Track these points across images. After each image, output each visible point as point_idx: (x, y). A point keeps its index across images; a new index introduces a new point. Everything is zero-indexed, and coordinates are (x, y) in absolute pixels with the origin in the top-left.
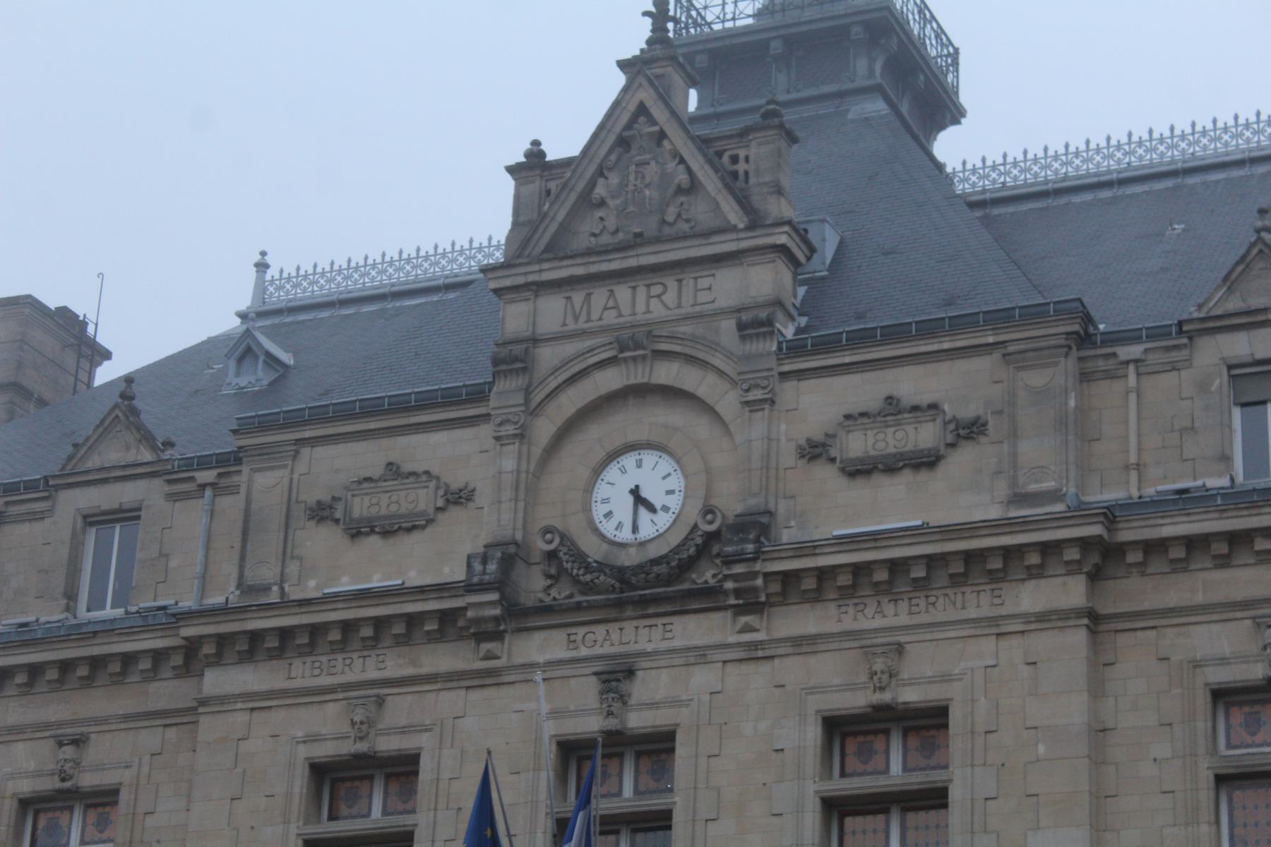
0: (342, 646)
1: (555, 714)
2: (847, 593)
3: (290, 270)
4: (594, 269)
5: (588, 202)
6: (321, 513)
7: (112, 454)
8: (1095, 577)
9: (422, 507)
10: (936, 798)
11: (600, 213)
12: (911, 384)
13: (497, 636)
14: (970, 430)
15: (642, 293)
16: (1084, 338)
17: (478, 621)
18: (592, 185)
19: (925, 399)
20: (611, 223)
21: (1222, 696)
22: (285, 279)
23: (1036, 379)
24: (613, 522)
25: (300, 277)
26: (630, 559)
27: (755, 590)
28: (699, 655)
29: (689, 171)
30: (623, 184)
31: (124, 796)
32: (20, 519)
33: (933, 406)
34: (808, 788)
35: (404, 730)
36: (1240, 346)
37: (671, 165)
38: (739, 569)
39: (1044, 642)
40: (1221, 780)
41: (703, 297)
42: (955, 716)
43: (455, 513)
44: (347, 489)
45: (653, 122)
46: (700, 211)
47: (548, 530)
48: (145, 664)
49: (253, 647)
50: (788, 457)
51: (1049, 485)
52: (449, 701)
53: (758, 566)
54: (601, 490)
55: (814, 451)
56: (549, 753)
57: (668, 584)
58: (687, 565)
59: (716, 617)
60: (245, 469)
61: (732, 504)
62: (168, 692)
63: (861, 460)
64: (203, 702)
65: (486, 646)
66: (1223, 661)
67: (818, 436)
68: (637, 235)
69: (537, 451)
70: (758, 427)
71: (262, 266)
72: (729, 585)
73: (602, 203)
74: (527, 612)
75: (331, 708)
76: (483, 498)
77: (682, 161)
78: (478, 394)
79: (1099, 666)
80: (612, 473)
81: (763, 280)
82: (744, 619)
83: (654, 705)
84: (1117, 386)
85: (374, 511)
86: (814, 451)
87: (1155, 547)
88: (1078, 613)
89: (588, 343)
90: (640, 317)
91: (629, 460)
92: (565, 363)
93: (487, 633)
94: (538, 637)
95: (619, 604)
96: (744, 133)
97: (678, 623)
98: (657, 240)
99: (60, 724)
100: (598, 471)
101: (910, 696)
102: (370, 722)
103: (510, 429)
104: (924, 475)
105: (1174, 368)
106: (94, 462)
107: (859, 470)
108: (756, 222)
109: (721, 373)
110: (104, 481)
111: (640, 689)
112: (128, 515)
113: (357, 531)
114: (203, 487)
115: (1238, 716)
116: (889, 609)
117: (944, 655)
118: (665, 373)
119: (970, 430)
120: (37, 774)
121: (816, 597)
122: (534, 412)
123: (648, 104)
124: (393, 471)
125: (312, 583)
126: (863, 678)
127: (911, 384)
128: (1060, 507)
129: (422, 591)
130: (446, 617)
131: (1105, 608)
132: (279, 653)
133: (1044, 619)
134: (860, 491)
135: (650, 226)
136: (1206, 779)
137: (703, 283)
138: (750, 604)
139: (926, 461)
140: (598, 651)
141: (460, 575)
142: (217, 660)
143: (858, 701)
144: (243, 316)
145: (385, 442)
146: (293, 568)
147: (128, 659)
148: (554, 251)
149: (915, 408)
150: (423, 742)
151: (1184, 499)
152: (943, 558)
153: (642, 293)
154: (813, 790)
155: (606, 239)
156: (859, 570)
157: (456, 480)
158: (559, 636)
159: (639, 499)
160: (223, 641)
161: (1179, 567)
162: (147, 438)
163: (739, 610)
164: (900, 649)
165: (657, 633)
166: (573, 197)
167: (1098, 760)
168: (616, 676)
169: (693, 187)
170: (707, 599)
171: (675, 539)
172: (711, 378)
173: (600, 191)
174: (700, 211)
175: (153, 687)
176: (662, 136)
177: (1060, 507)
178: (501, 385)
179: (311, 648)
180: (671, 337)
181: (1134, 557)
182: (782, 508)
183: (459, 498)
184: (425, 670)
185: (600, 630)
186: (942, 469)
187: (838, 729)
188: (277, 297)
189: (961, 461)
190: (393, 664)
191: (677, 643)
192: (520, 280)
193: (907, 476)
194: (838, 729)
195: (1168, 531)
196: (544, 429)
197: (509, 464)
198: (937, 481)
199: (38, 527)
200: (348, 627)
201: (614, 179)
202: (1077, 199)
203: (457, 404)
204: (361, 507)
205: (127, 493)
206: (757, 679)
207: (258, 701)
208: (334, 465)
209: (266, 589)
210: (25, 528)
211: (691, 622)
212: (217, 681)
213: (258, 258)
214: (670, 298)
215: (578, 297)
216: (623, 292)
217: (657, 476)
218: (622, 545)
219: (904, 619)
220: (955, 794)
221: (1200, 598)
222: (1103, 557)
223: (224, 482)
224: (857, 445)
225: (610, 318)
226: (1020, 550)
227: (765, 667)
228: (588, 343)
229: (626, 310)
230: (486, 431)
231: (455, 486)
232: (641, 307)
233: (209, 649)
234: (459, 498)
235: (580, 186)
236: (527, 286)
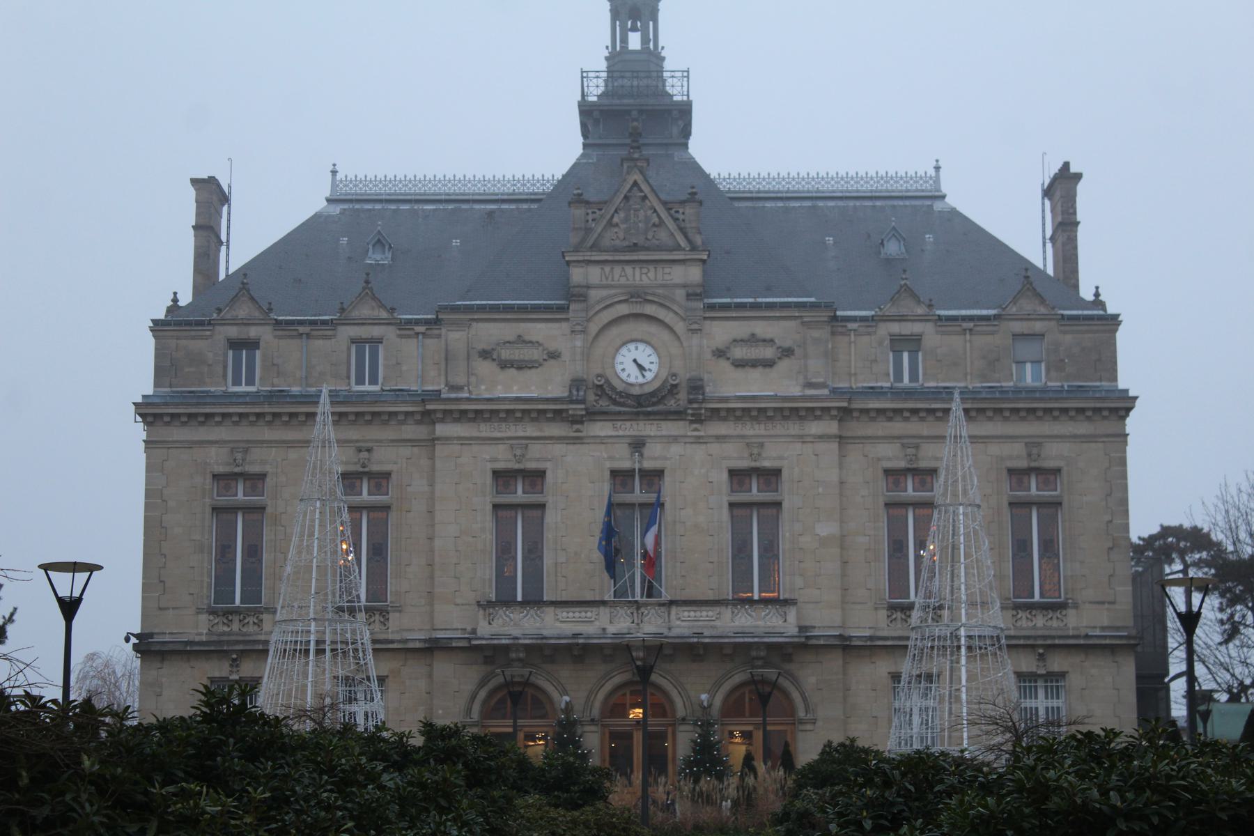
0: (504, 420)
1: (611, 458)
2: (738, 419)
3: (351, 176)
4: (617, 258)
5: (610, 224)
7: (365, 311)
8: (840, 421)
9: (536, 357)
10: (778, 505)
11: (616, 230)
12: (762, 329)
13: (582, 422)
14: (787, 352)
15: (637, 271)
16: (835, 318)
17: (573, 416)
18: (612, 216)
19: (768, 336)
20: (621, 235)
21: (887, 472)
22: (346, 182)
23: (816, 334)
25: (356, 182)
26: (636, 391)
28: (675, 439)
30: (626, 220)
31: (394, 476)
32: (317, 338)
33: (772, 341)
34: (723, 496)
35: (538, 460)
36: (895, 328)
37: (649, 212)
38: (695, 406)
39: (821, 447)
40: (886, 504)
41: (667, 277)
42: (785, 474)
43: (552, 362)
44: (498, 344)
45: (641, 191)
46: (663, 235)
47: (598, 376)
48: (401, 417)
49: (462, 417)
50: (709, 356)
51: (821, 380)
52: (558, 449)
53: (704, 405)
54: (619, 358)
55: (720, 353)
56: (607, 474)
57: (654, 404)
58: (663, 397)
59: (681, 423)
60: (443, 331)
61: (684, 376)
62: (411, 431)
63: (741, 360)
64: (438, 439)
65: (576, 427)
66: (889, 459)
67: (721, 347)
68: (635, 244)
69: (590, 339)
70: (695, 340)
71: (334, 172)
72: (690, 411)
73: (617, 225)
74: (594, 413)
75: (501, 447)
76: (566, 356)
77: (655, 211)
78: (561, 309)
79: (842, 456)
80: (624, 351)
81: (694, 274)
82: (695, 426)
83: (655, 459)
84: (846, 339)
85: (512, 357)
86: (720, 353)
87: (865, 411)
88: (835, 436)
89: (613, 292)
91: (632, 346)
92: (603, 299)
93: (576, 421)
94: (599, 424)
95: (638, 414)
96: (683, 202)
97: (664, 424)
98: (647, 249)
99: (357, 441)
100: (617, 350)
101: (767, 464)
102: (523, 456)
103: (579, 328)
104: (767, 370)
105: (869, 334)
106: (355, 314)
107: (740, 364)
108: (694, 248)
109: (676, 313)
110: (363, 324)
111: (647, 451)
112: (376, 342)
113: (504, 365)
114: (418, 334)
115: (891, 479)
116: (756, 426)
117: (782, 448)
118: (649, 309)
119: (787, 352)
120: (346, 463)
121: (725, 419)
122: (589, 320)
123: (639, 182)
124: (520, 340)
126: (746, 455)
127: (762, 329)
128: (826, 392)
129: (548, 400)
130: (556, 412)
131: (844, 434)
132: (473, 420)
133: (822, 437)
134: (740, 374)
135: (640, 240)
136: (881, 504)
137: (667, 270)
138: (698, 419)
139: (769, 364)
140: (627, 433)
142: (442, 421)
143: (745, 464)
144: (328, 200)
145: (514, 325)
146: (473, 379)
147: (391, 414)
148: (595, 247)
149: (764, 341)
150: (548, 465)
151: (873, 392)
152: (781, 409)
153: (637, 271)
154: (725, 500)
155: (617, 242)
156: (743, 409)
157: (552, 346)
158: (609, 424)
159: (641, 368)
160: (445, 411)
161: (873, 419)
162: (383, 306)
163: (692, 422)
164: (762, 445)
165: (654, 427)
166: (605, 222)
167: (841, 495)
168: (638, 445)
169: (662, 223)
170: (678, 415)
171: (657, 385)
172: (671, 315)
173: (616, 220)
174: (663, 235)
175: (404, 427)
176: (645, 198)
177: (826, 392)
179: (489, 420)
180: (654, 294)
181: (855, 414)
182: (706, 377)
183: (554, 355)
184: (546, 434)
185: (628, 424)
186: (776, 368)
187: (733, 473)
188: (343, 190)
189: (784, 365)
190: (530, 430)
191: (664, 433)
192: (581, 258)
193: (760, 369)
194: (733, 473)
195: (871, 406)
196: (594, 328)
197: (579, 343)
198: (773, 373)
199: (328, 342)
200: (508, 412)
201: (622, 215)
202: (768, 204)
203: (556, 312)
204: (506, 354)
205: (376, 331)
206: (699, 452)
207: (464, 441)
208: (490, 332)
209: (460, 388)
210: (321, 342)
211: (670, 424)
212: (441, 429)
213: (331, 168)
214: (651, 275)
215: (607, 269)
216: (629, 270)
217: (644, 354)
218: (631, 385)
219: (763, 432)
220: (785, 505)
221: (880, 433)
222: (845, 414)
223: (429, 332)
224: (739, 353)
225: (623, 281)
226: (813, 409)
227: (703, 447)
228: (613, 292)
229: (631, 278)
230: (564, 325)
231: (551, 349)
232: (637, 278)
233: (439, 415)
234: (554, 355)
235: (608, 217)
236: (583, 261)
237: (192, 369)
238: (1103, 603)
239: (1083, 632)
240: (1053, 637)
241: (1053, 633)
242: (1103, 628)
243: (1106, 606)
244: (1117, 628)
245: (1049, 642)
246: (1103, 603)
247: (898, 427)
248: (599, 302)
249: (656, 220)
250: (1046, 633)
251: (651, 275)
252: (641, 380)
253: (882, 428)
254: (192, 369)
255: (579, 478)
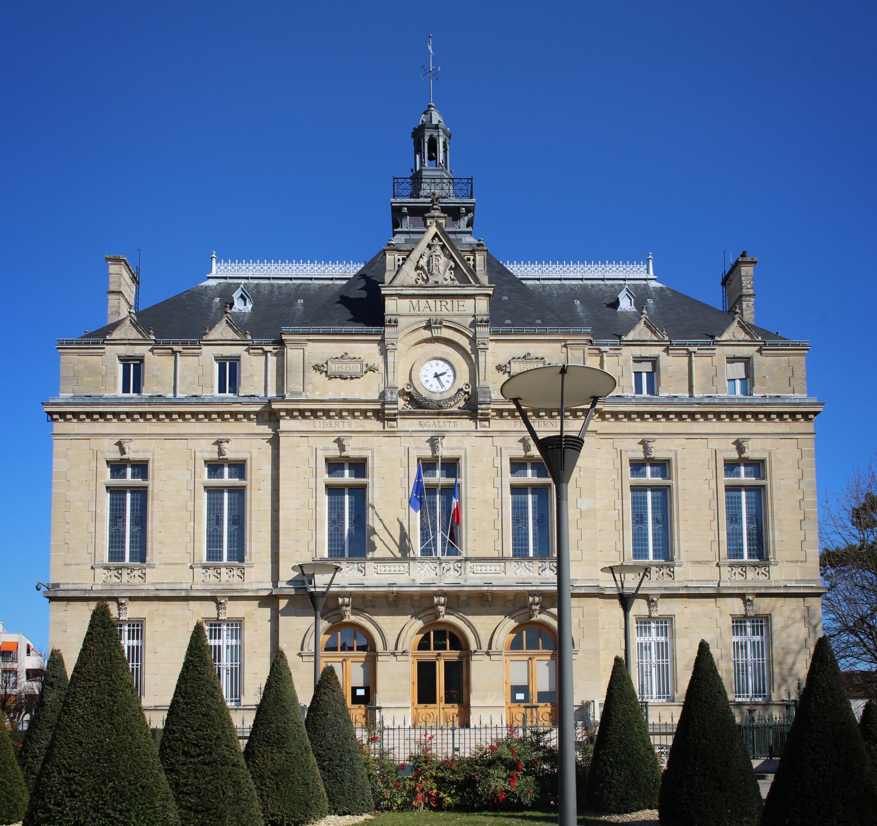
6: (317, 368)
12: (536, 349)
24: (429, 384)
27: (488, 414)
29: (454, 261)
33: (542, 358)
45: (441, 241)
67: (503, 364)
68: (436, 282)
85: (341, 370)
89: (419, 319)
90: (438, 312)
95: (439, 414)
125: (317, 393)
141: (377, 398)
145: (342, 345)
178: (387, 330)
192: (394, 292)
204: (333, 368)
209: (300, 394)
215: (415, 301)
216: (431, 302)
225: (427, 311)
229: (433, 308)
232: (438, 309)
236: (396, 295)
237: (90, 379)
238: (797, 562)
239: (782, 584)
240: (760, 588)
241: (760, 585)
242: (797, 581)
243: (800, 564)
244: (808, 581)
245: (757, 591)
246: (797, 562)
247: (638, 426)
248: (407, 327)
249: (452, 264)
250: (754, 584)
251: (449, 306)
252: (440, 390)
253: (626, 426)
254: (90, 379)
255: (392, 464)
